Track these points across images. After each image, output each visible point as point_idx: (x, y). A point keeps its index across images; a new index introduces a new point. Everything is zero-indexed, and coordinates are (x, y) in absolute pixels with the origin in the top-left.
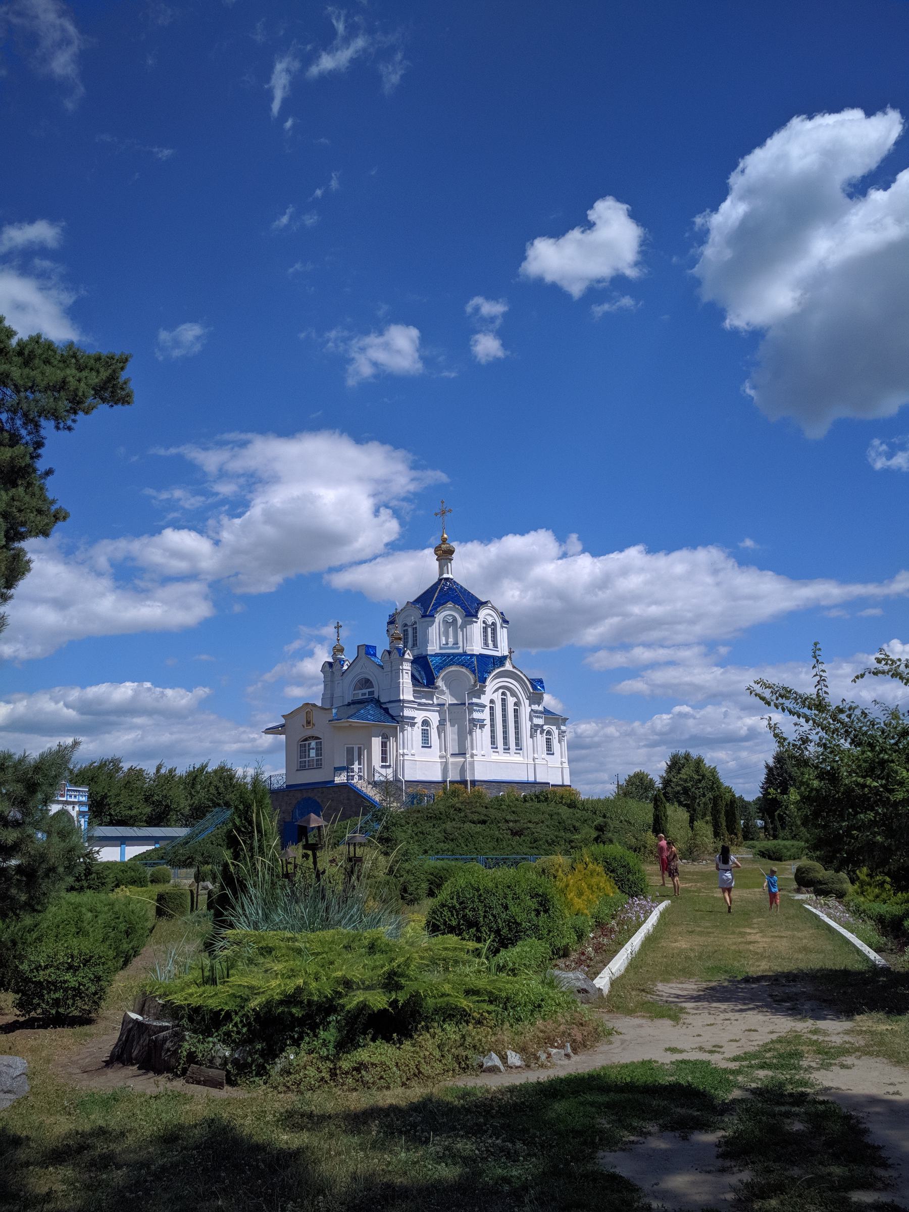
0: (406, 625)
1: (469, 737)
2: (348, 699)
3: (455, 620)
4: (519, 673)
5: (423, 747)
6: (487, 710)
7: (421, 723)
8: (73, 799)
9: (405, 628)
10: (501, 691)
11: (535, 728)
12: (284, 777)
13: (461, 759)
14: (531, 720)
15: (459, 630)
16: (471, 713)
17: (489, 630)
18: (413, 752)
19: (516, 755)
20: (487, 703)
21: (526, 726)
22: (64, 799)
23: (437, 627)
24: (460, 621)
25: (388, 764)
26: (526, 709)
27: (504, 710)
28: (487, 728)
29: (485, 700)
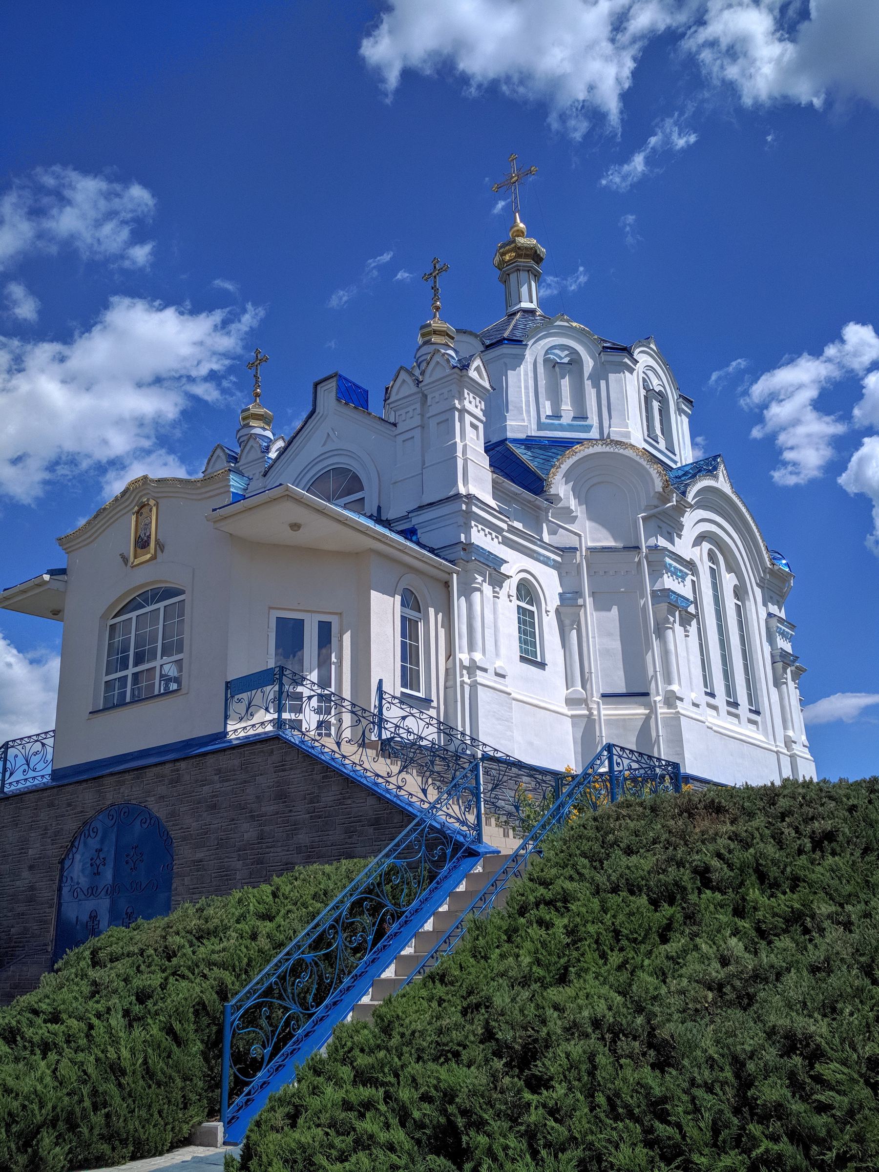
1: (656, 644)
3: (576, 361)
12: (50, 742)
13: (635, 711)
14: (771, 640)
15: (588, 383)
16: (656, 574)
18: (499, 664)
23: (531, 374)
24: (589, 364)
25: (421, 695)
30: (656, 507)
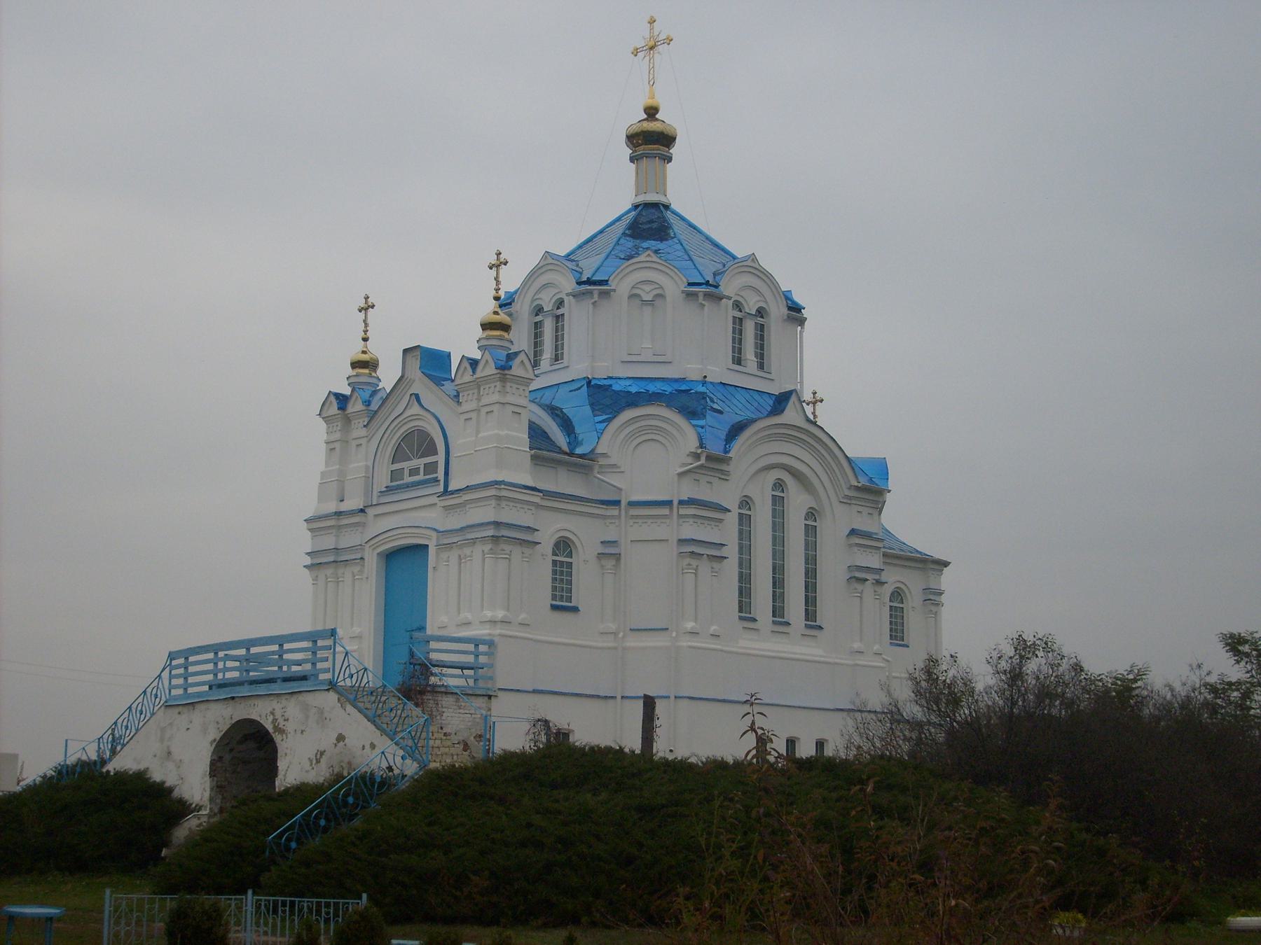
0: (539, 310)
5: (554, 608)
6: (732, 519)
9: (539, 318)
11: (857, 576)
17: (749, 328)
20: (731, 502)
27: (779, 526)
28: (731, 568)
30: (691, 464)
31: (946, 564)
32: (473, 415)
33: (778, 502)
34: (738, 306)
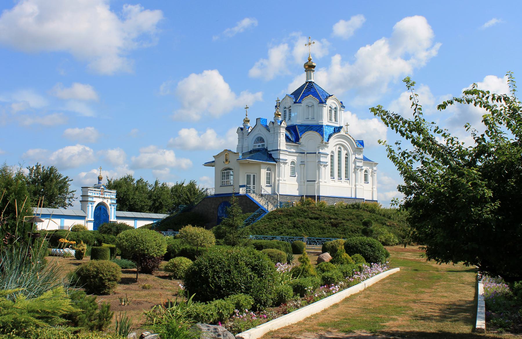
0: (285, 108)
2: (251, 149)
4: (349, 137)
5: (290, 176)
6: (329, 157)
7: (290, 163)
8: (108, 197)
9: (285, 110)
10: (338, 146)
11: (356, 168)
12: (214, 189)
17: (333, 112)
19: (345, 183)
20: (330, 154)
21: (352, 166)
22: (103, 196)
26: (352, 158)
28: (329, 167)
29: (327, 151)
31: (377, 164)
32: (273, 134)
33: (340, 152)
34: (330, 107)
